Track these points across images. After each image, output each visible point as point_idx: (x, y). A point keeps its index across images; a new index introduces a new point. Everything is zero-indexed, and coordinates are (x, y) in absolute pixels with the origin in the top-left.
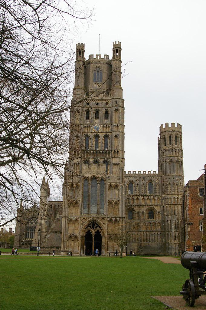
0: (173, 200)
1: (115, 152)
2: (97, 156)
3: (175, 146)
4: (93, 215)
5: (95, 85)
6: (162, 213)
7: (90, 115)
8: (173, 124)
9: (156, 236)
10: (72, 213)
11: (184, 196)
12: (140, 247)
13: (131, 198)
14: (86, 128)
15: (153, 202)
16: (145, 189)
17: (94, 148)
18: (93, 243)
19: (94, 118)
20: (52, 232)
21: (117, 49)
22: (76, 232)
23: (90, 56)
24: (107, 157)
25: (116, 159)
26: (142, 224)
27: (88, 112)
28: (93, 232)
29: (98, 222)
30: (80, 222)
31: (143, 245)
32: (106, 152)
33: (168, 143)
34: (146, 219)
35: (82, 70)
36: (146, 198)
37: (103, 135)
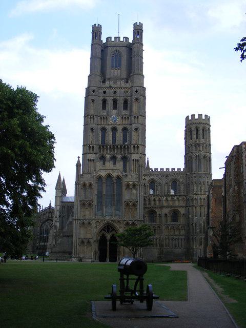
0: (199, 201)
1: (134, 147)
2: (114, 151)
3: (202, 141)
4: (107, 218)
5: (112, 71)
6: (186, 216)
7: (107, 105)
8: (200, 115)
9: (180, 241)
10: (85, 216)
11: (208, 197)
12: (161, 253)
13: (152, 198)
14: (103, 121)
15: (177, 203)
16: (168, 188)
18: (108, 248)
19: (112, 108)
20: (64, 236)
21: (138, 30)
22: (88, 236)
23: (107, 39)
24: (126, 152)
26: (164, 228)
27: (104, 101)
28: (108, 236)
29: (113, 225)
30: (94, 225)
31: (164, 251)
32: (125, 147)
33: (194, 137)
34: (169, 223)
35: (99, 55)
36: (169, 199)
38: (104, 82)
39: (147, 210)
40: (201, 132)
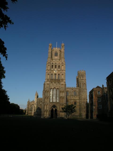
5: (55, 57)
15: (76, 98)
17: (54, 79)
25: (62, 82)
28: (54, 109)
37: (58, 74)
38: (52, 60)
40: (83, 75)
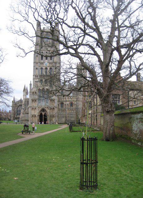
12: (66, 120)
22: (35, 114)
30: (37, 109)
31: (67, 119)
39: (60, 102)
